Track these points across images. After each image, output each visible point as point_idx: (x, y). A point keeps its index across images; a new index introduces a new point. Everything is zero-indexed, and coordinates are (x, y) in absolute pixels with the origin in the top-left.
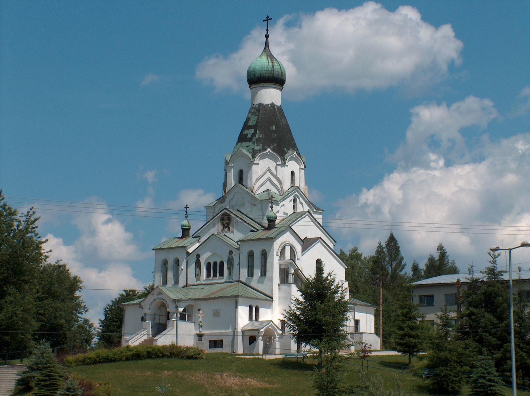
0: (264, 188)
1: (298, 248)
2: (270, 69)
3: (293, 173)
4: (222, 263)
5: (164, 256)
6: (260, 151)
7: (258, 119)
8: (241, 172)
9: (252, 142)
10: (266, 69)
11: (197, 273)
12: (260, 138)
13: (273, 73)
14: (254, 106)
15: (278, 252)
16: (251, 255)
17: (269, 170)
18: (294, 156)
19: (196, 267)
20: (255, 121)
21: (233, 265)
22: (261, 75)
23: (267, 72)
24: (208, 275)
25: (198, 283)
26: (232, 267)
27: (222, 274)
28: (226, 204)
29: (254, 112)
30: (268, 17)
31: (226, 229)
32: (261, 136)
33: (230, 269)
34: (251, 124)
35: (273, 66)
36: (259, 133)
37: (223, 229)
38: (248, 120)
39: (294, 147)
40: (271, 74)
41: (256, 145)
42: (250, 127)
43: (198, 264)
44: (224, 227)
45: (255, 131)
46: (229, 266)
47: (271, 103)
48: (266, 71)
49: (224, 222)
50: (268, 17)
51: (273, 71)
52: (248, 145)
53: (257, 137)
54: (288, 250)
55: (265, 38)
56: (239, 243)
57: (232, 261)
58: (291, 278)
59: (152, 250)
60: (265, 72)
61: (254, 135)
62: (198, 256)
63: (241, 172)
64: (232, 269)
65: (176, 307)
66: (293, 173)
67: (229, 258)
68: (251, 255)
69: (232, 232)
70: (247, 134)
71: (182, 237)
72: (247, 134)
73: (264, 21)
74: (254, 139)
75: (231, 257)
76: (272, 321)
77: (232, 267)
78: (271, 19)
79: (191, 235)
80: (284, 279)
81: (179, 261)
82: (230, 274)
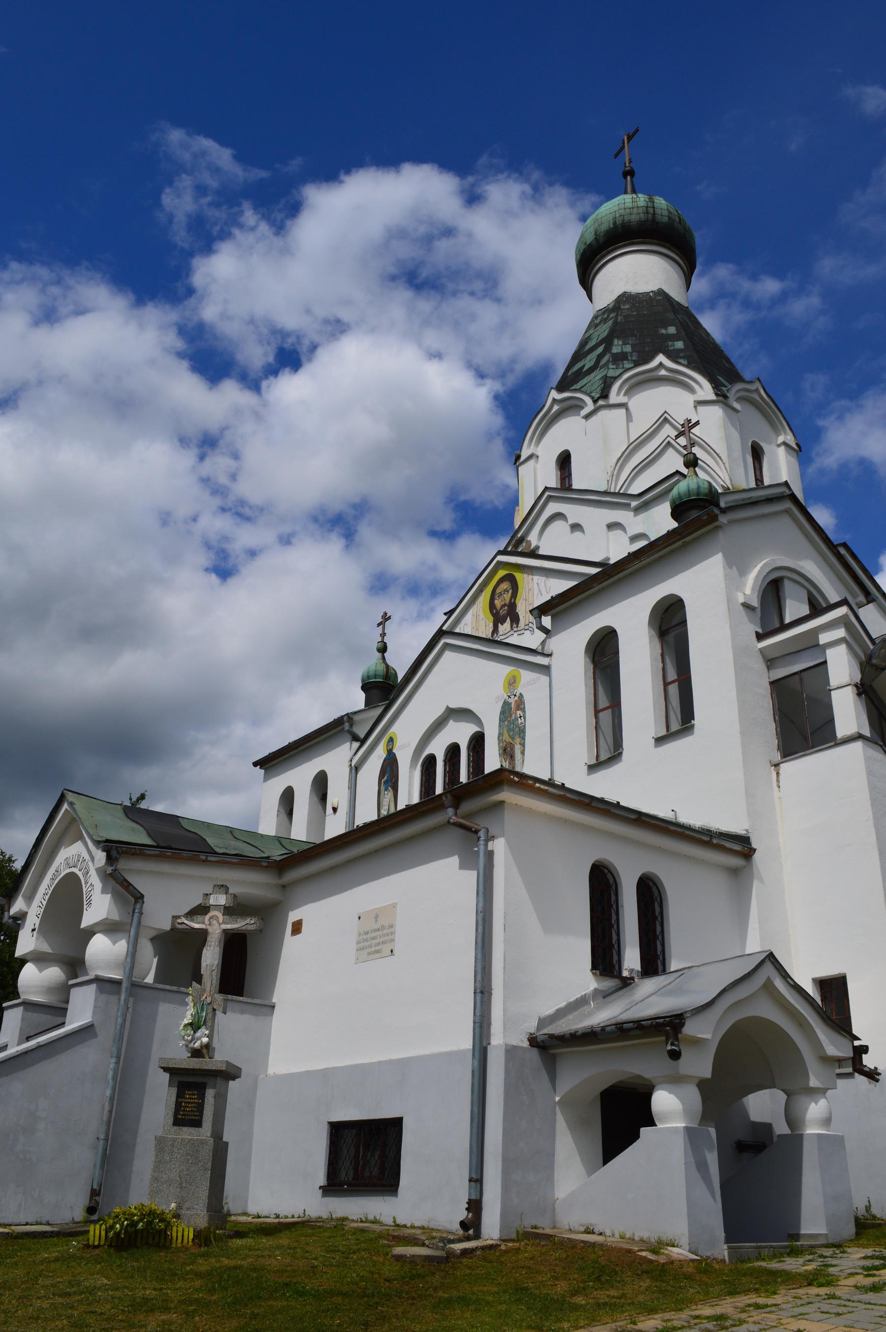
8: (564, 461)
12: (626, 353)
13: (654, 214)
19: (383, 788)
21: (522, 732)
22: (615, 223)
23: (635, 210)
26: (518, 740)
31: (507, 626)
32: (628, 349)
36: (620, 343)
37: (495, 630)
40: (647, 213)
44: (498, 620)
46: (506, 737)
49: (498, 603)
51: (654, 207)
57: (519, 712)
59: (255, 764)
60: (628, 211)
64: (518, 749)
67: (506, 705)
75: (512, 700)
77: (518, 740)
78: (637, 130)
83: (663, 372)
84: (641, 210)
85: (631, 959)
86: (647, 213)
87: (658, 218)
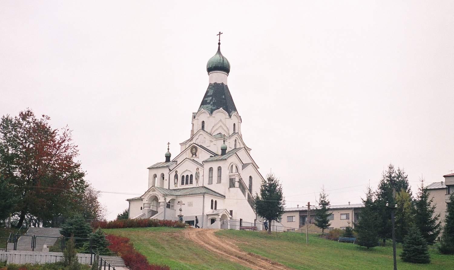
0: (218, 132)
1: (240, 167)
2: (221, 62)
3: (234, 124)
4: (192, 176)
5: (154, 172)
6: (215, 110)
7: (214, 91)
8: (203, 122)
9: (210, 105)
10: (219, 62)
11: (175, 182)
14: (211, 85)
15: (229, 168)
16: (211, 169)
17: (221, 120)
18: (236, 114)
20: (212, 93)
21: (199, 177)
24: (183, 184)
25: (176, 188)
27: (191, 183)
28: (194, 141)
29: (211, 88)
30: (220, 32)
32: (216, 101)
33: (196, 179)
34: (209, 95)
35: (223, 60)
37: (192, 156)
38: (207, 92)
39: (235, 110)
40: (222, 64)
41: (213, 106)
42: (209, 96)
43: (176, 176)
44: (193, 154)
45: (212, 98)
47: (221, 83)
48: (219, 63)
49: (193, 152)
50: (220, 32)
52: (208, 106)
53: (213, 101)
54: (234, 167)
55: (218, 45)
56: (204, 163)
58: (237, 184)
61: (211, 100)
62: (176, 172)
63: (203, 122)
65: (164, 199)
66: (234, 124)
67: (196, 172)
68: (211, 169)
69: (198, 157)
70: (207, 100)
71: (166, 162)
72: (207, 100)
73: (217, 35)
74: (211, 103)
75: (198, 172)
76: (226, 210)
78: (222, 33)
79: (171, 160)
80: (232, 184)
81: (164, 175)
82: (197, 182)
83: (222, 111)
84: (221, 64)
85: (214, 208)
86: (222, 64)
87: (224, 66)
